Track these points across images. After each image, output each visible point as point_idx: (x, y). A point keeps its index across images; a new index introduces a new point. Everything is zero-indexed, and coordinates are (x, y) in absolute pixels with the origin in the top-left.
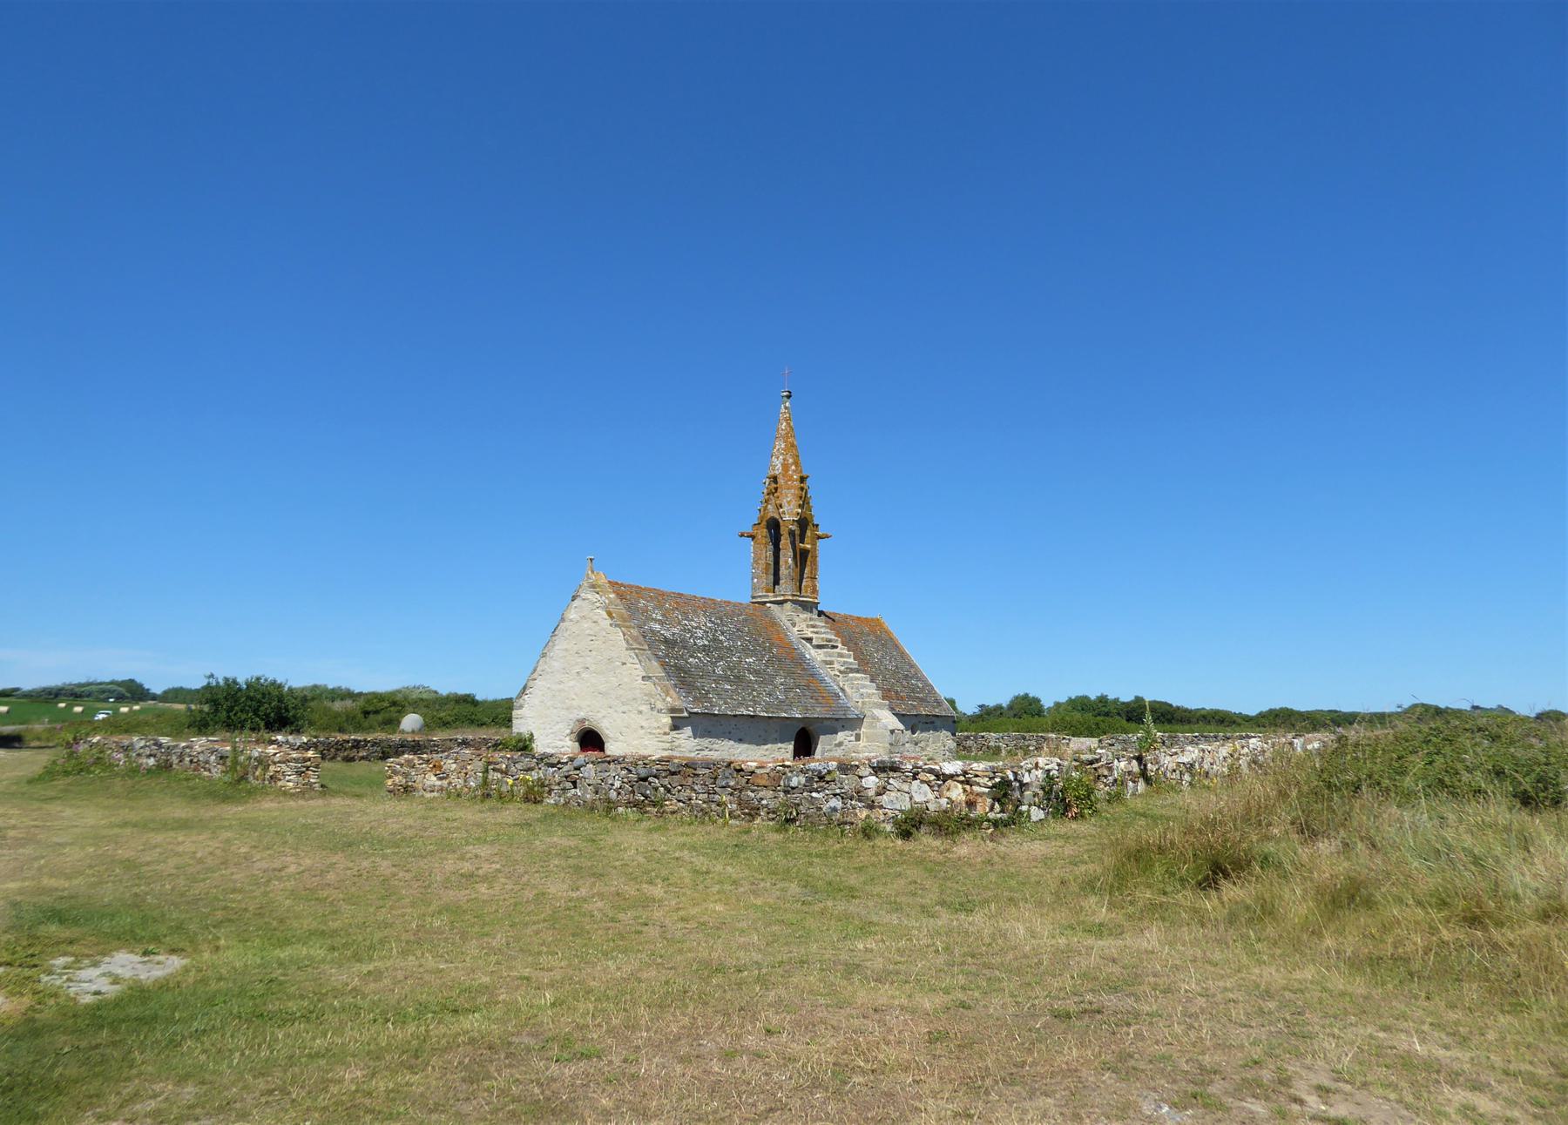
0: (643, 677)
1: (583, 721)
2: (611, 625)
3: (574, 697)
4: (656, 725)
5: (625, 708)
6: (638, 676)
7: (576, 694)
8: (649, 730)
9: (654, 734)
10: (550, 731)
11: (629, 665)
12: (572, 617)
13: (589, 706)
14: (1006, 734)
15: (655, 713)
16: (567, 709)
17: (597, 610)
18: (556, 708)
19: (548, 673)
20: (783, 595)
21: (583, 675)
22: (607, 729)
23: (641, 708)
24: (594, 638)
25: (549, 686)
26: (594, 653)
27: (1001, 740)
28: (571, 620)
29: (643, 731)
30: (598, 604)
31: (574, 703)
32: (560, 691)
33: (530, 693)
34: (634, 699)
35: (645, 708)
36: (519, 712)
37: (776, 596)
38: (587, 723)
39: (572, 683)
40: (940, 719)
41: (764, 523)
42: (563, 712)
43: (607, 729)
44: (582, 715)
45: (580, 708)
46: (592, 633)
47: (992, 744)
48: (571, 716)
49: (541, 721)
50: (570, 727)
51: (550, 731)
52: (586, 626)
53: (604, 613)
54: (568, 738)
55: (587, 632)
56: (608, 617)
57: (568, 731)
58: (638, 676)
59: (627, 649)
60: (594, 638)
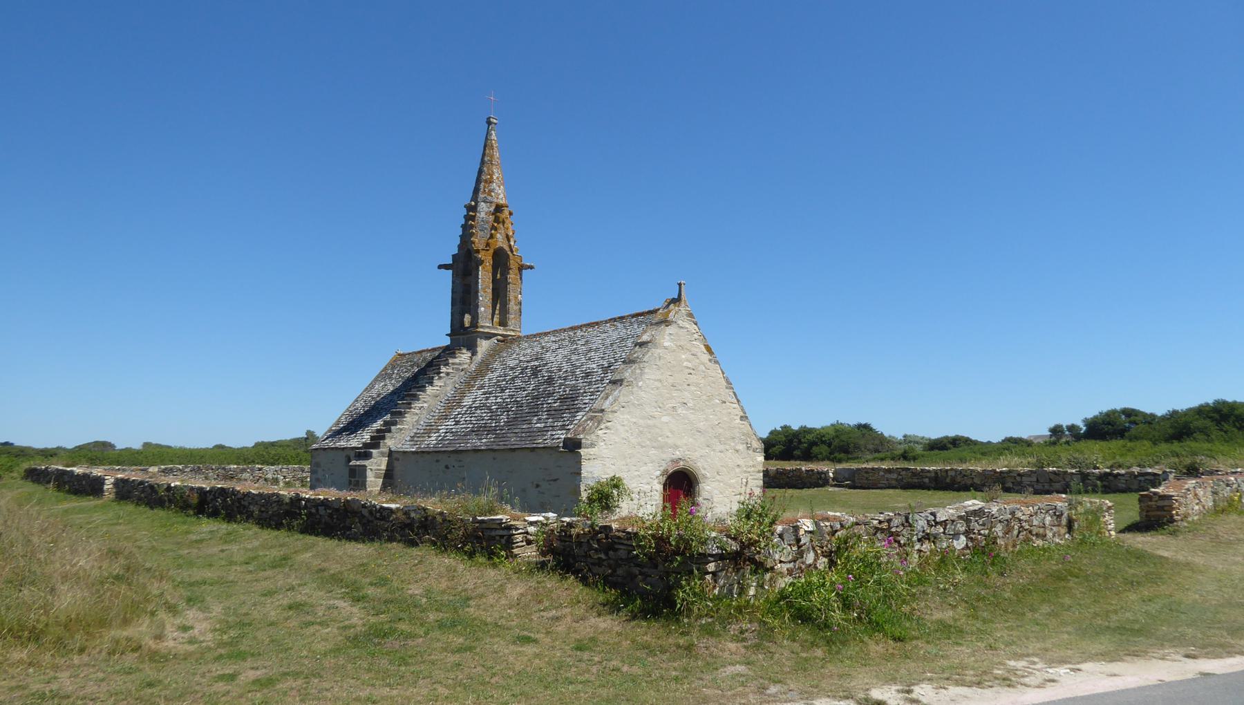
0: (742, 417)
1: (676, 461)
2: (710, 360)
3: (669, 434)
4: (751, 463)
5: (722, 447)
6: (737, 415)
7: (672, 432)
8: (745, 469)
9: (749, 472)
10: (637, 473)
11: (727, 403)
12: (666, 344)
13: (686, 445)
14: (285, 466)
15: (751, 452)
16: (662, 447)
17: (694, 343)
18: (642, 447)
19: (633, 404)
20: (513, 331)
21: (680, 411)
22: (705, 469)
23: (737, 448)
24: (692, 371)
25: (634, 420)
26: (692, 388)
27: (279, 472)
28: (666, 348)
29: (737, 470)
30: (696, 336)
31: (670, 441)
32: (649, 426)
33: (607, 428)
34: (733, 438)
35: (741, 447)
36: (591, 451)
37: (507, 330)
38: (682, 463)
39: (665, 419)
40: (480, 453)
41: (491, 251)
42: (653, 451)
43: (705, 469)
44: (678, 454)
45: (676, 447)
46: (690, 365)
47: (270, 476)
48: (664, 456)
49: (624, 463)
50: (662, 469)
51: (637, 473)
52: (683, 357)
53: (702, 346)
54: (656, 481)
55: (685, 364)
56: (705, 351)
57: (658, 473)
58: (737, 415)
59: (727, 388)
60: (692, 371)
